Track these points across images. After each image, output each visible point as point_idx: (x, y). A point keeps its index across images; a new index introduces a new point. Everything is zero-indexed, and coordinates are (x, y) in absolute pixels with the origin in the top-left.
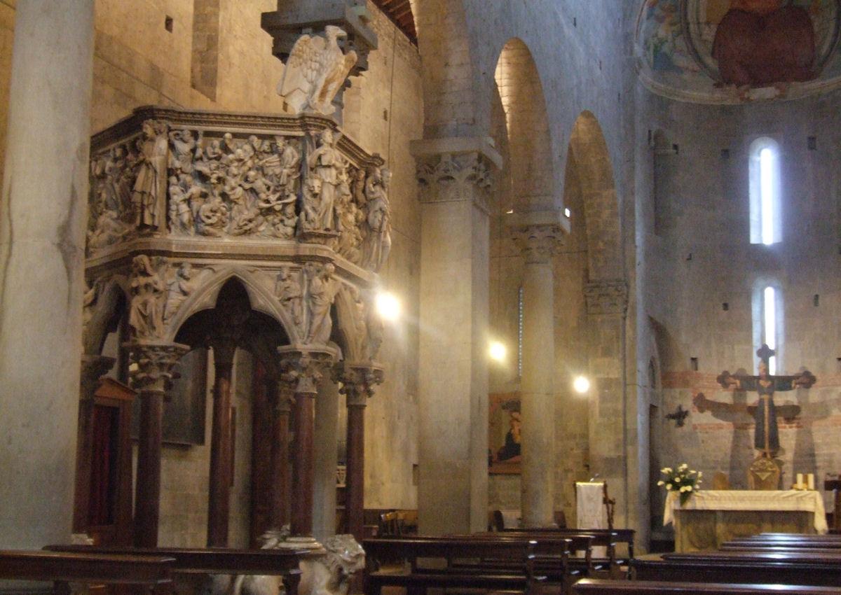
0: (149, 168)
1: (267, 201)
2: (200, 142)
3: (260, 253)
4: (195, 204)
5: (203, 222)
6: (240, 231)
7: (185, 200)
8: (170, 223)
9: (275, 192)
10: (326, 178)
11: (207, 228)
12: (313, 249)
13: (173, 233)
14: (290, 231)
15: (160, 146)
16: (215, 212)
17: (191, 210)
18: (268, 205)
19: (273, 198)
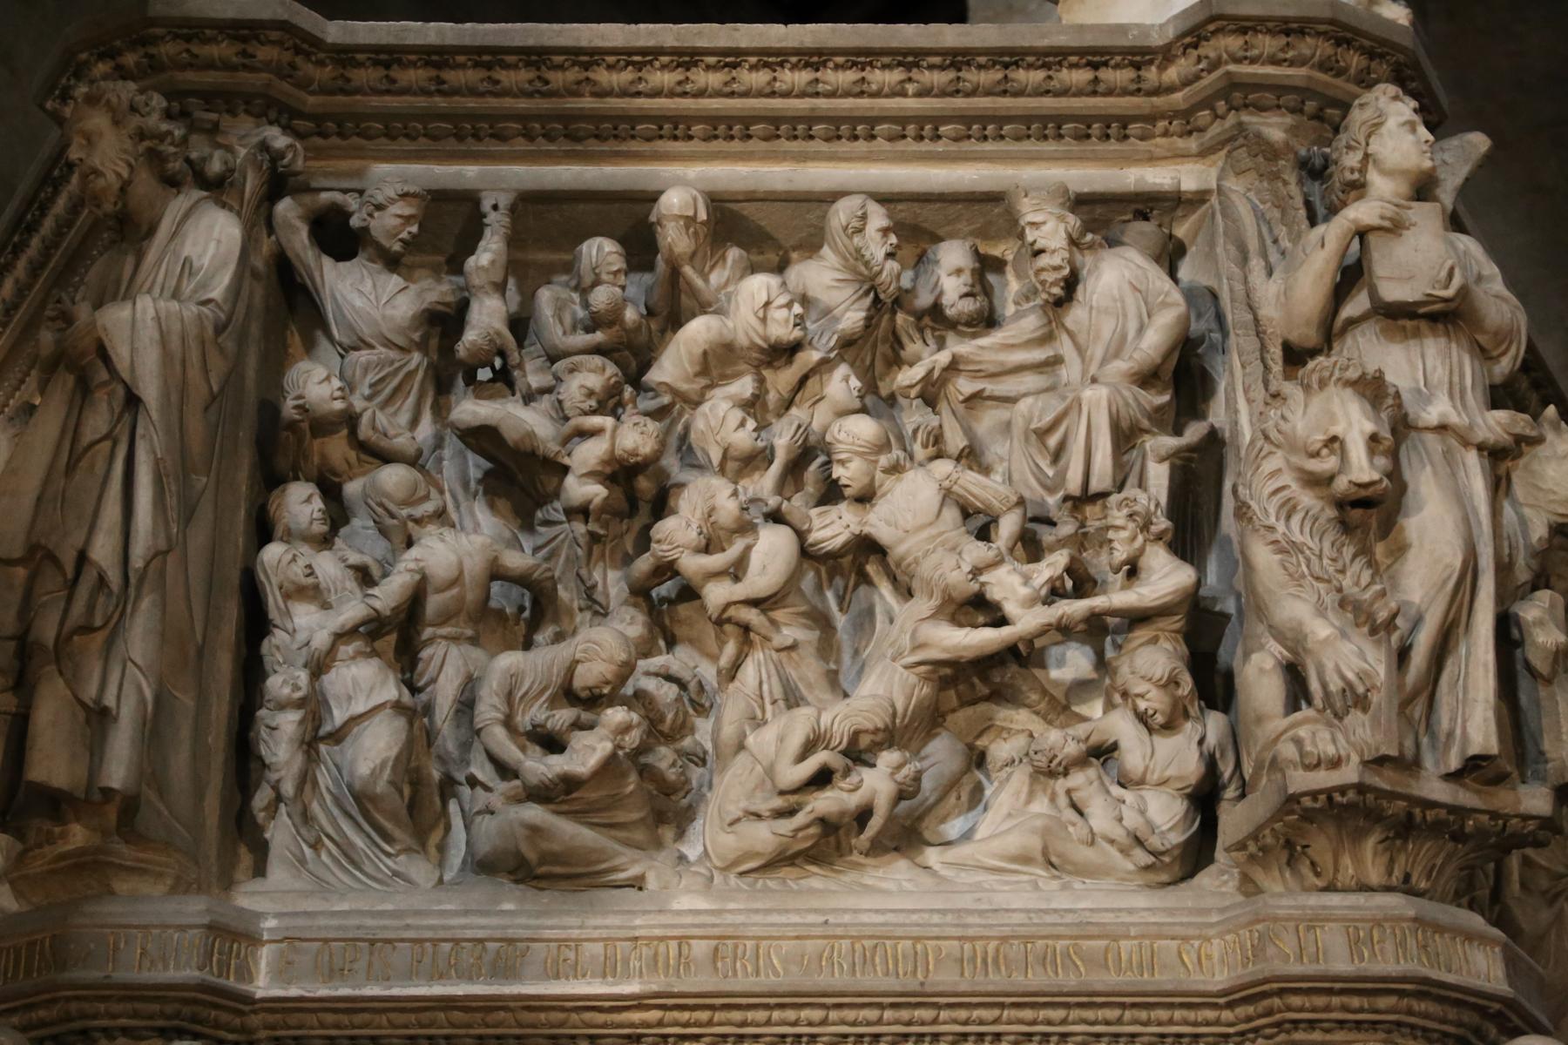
0: (84, 390)
1: (978, 607)
2: (488, 255)
3: (945, 978)
4: (448, 664)
5: (505, 770)
6: (786, 826)
7: (371, 630)
8: (261, 798)
9: (1030, 546)
10: (1426, 399)
11: (534, 813)
12: (1378, 923)
13: (278, 873)
14: (1165, 814)
15: (188, 250)
16: (593, 701)
17: (428, 709)
18: (983, 638)
19: (1012, 586)
